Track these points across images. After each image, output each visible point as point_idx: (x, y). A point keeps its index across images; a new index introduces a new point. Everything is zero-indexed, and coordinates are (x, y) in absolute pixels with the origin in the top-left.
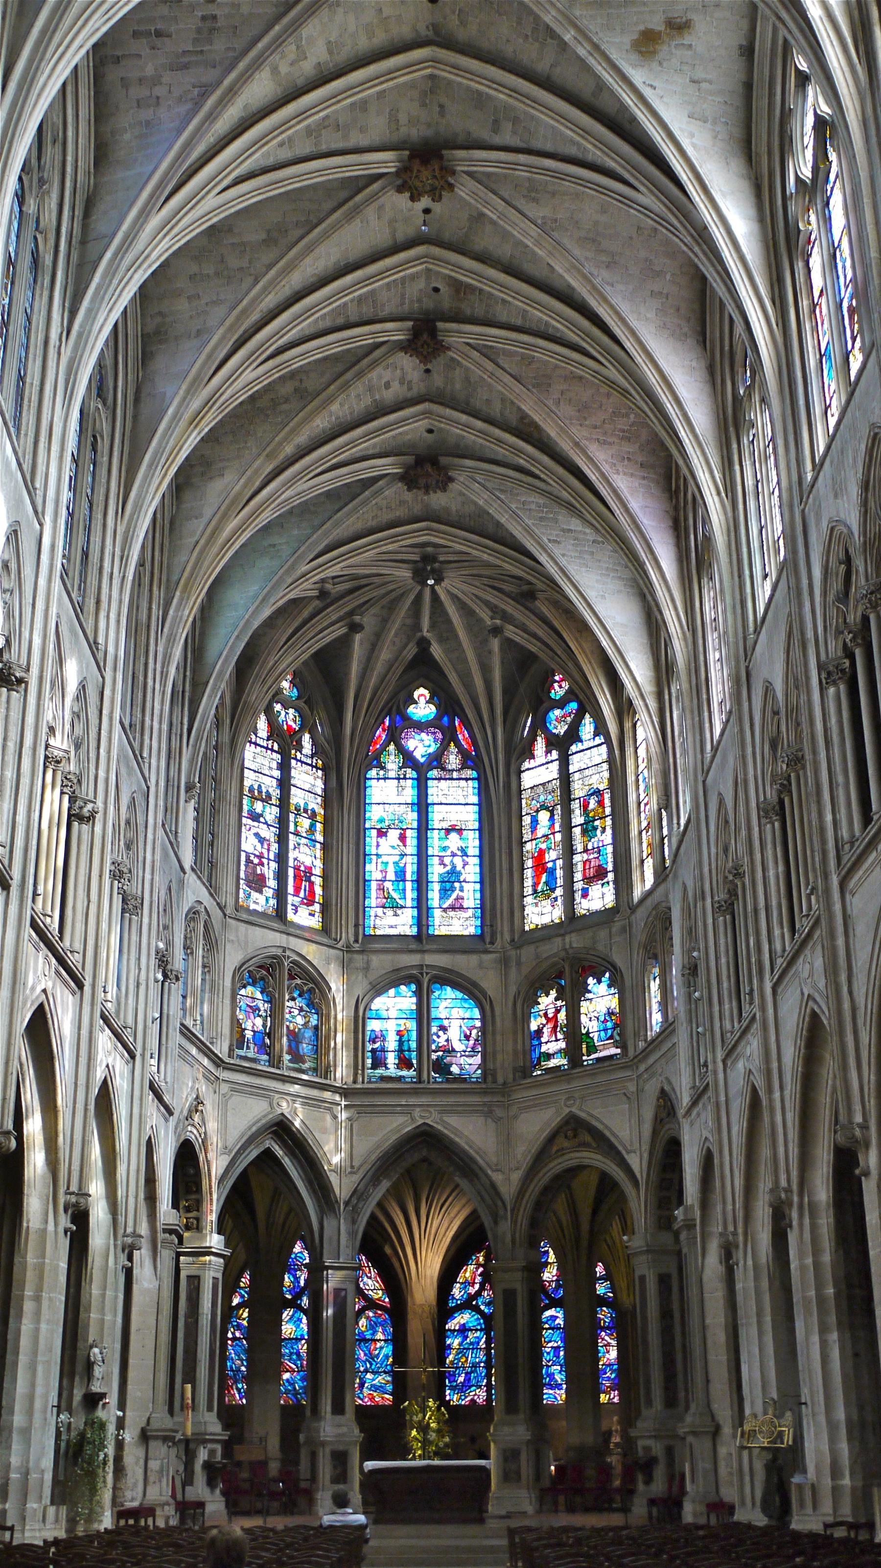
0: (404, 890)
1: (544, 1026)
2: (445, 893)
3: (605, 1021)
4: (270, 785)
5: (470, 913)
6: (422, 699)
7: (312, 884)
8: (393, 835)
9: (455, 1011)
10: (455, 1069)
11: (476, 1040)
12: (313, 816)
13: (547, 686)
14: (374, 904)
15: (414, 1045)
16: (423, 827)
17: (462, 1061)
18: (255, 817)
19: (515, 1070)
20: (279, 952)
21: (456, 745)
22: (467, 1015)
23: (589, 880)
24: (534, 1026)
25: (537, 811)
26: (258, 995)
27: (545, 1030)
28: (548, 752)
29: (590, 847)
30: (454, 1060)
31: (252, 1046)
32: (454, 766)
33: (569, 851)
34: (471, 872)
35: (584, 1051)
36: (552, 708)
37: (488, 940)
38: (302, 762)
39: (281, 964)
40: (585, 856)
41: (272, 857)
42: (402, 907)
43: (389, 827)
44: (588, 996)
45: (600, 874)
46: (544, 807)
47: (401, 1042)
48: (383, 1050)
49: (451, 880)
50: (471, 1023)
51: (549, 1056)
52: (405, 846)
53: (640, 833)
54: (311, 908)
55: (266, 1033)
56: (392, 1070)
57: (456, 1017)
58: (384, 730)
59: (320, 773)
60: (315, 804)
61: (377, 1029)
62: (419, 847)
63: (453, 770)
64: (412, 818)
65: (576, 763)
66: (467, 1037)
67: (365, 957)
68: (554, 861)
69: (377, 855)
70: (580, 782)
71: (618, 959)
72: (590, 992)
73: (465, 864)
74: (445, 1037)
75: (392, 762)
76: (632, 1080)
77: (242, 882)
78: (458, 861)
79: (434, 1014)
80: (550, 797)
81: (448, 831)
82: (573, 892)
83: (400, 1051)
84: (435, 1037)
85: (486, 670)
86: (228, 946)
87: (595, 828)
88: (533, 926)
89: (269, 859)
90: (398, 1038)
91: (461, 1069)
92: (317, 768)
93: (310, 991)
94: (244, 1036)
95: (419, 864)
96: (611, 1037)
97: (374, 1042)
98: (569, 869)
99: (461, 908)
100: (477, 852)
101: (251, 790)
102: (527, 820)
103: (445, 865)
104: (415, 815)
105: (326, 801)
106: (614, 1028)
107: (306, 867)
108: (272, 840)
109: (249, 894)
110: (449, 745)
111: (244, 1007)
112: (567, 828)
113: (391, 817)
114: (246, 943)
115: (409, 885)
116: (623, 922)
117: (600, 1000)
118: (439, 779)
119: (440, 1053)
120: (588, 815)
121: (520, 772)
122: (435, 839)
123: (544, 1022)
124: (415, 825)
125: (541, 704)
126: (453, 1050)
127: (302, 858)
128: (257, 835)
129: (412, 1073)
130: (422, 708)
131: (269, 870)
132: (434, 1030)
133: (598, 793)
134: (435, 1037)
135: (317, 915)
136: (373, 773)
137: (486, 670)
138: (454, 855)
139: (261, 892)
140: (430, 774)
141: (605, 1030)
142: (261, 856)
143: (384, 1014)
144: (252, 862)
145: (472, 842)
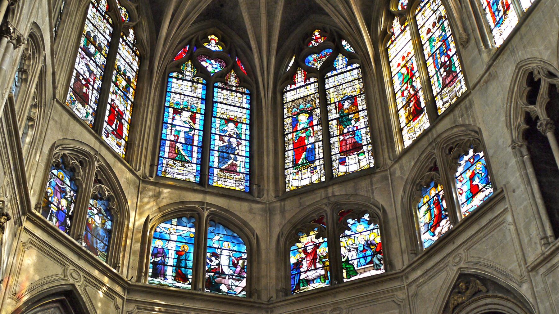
0: (192, 151)
1: (304, 259)
2: (222, 160)
3: (364, 250)
4: (103, 39)
5: (241, 176)
6: (213, 42)
7: (122, 125)
8: (186, 115)
9: (226, 244)
10: (223, 288)
11: (242, 268)
12: (128, 81)
13: (306, 41)
14: (166, 155)
15: (190, 264)
16: (209, 115)
17: (230, 282)
18: (90, 55)
19: (277, 291)
20: (92, 153)
21: (235, 72)
22: (235, 248)
23: (345, 153)
24: (293, 260)
25: (298, 114)
26: (68, 182)
27: (304, 262)
28: (307, 78)
29: (345, 131)
30: (223, 280)
31: (55, 219)
32: (233, 84)
33: (327, 135)
34: (244, 149)
35: (345, 275)
36: (311, 54)
37: (256, 194)
38: (127, 44)
39: (91, 163)
40: (342, 138)
41: (96, 86)
42: (189, 162)
43: (183, 109)
44: (347, 232)
45: (356, 147)
46: (303, 111)
47: (179, 260)
48: (164, 264)
49: (227, 152)
50: (238, 255)
51: (308, 282)
52: (194, 123)
53: (397, 112)
54: (119, 140)
55: (69, 216)
56: (169, 280)
57: (225, 251)
58: (185, 52)
59: (137, 59)
60: (131, 75)
61: (160, 247)
62: (204, 125)
63: (233, 86)
64: (201, 107)
65: (330, 83)
66: (235, 265)
67: (157, 189)
68: (313, 144)
69: (172, 124)
70: (336, 93)
71: (380, 199)
72: (349, 229)
73: (239, 144)
74: (217, 262)
75: (189, 72)
76: (402, 288)
77: (70, 89)
78: (233, 140)
79: (209, 243)
80: (309, 105)
81: (228, 121)
82: (331, 162)
83: (178, 267)
84: (208, 261)
85: (270, 15)
86: (51, 122)
87: (350, 120)
88: (292, 188)
89: (93, 88)
90: (176, 256)
91: (229, 289)
92: (136, 55)
93: (109, 199)
94: (50, 208)
95: (204, 136)
96: (371, 262)
97: (155, 255)
98: (327, 147)
99: (235, 171)
100: (248, 138)
101: (88, 33)
102: (288, 121)
103: (224, 142)
104: (203, 106)
105: (139, 75)
106: (373, 255)
107: (118, 109)
108: (98, 76)
109: (74, 102)
110: (230, 71)
111: (53, 184)
112: (324, 121)
113: (185, 103)
114: (67, 129)
115: (195, 149)
116: (383, 174)
117: (360, 234)
118: (223, 89)
119: (212, 274)
120: (343, 112)
121: (283, 93)
122: (217, 124)
123: (303, 255)
124: (203, 112)
125: (302, 52)
126: (223, 273)
127: (117, 102)
128: (87, 65)
129: (187, 286)
130: (213, 45)
131: (93, 96)
132: (208, 255)
133: (353, 99)
134: (208, 261)
135: (122, 148)
136: (175, 74)
137: (270, 15)
138: (230, 136)
139: (84, 106)
140: (216, 84)
141: (365, 257)
142: (88, 81)
143: (167, 237)
144: (81, 81)
145: (245, 131)
